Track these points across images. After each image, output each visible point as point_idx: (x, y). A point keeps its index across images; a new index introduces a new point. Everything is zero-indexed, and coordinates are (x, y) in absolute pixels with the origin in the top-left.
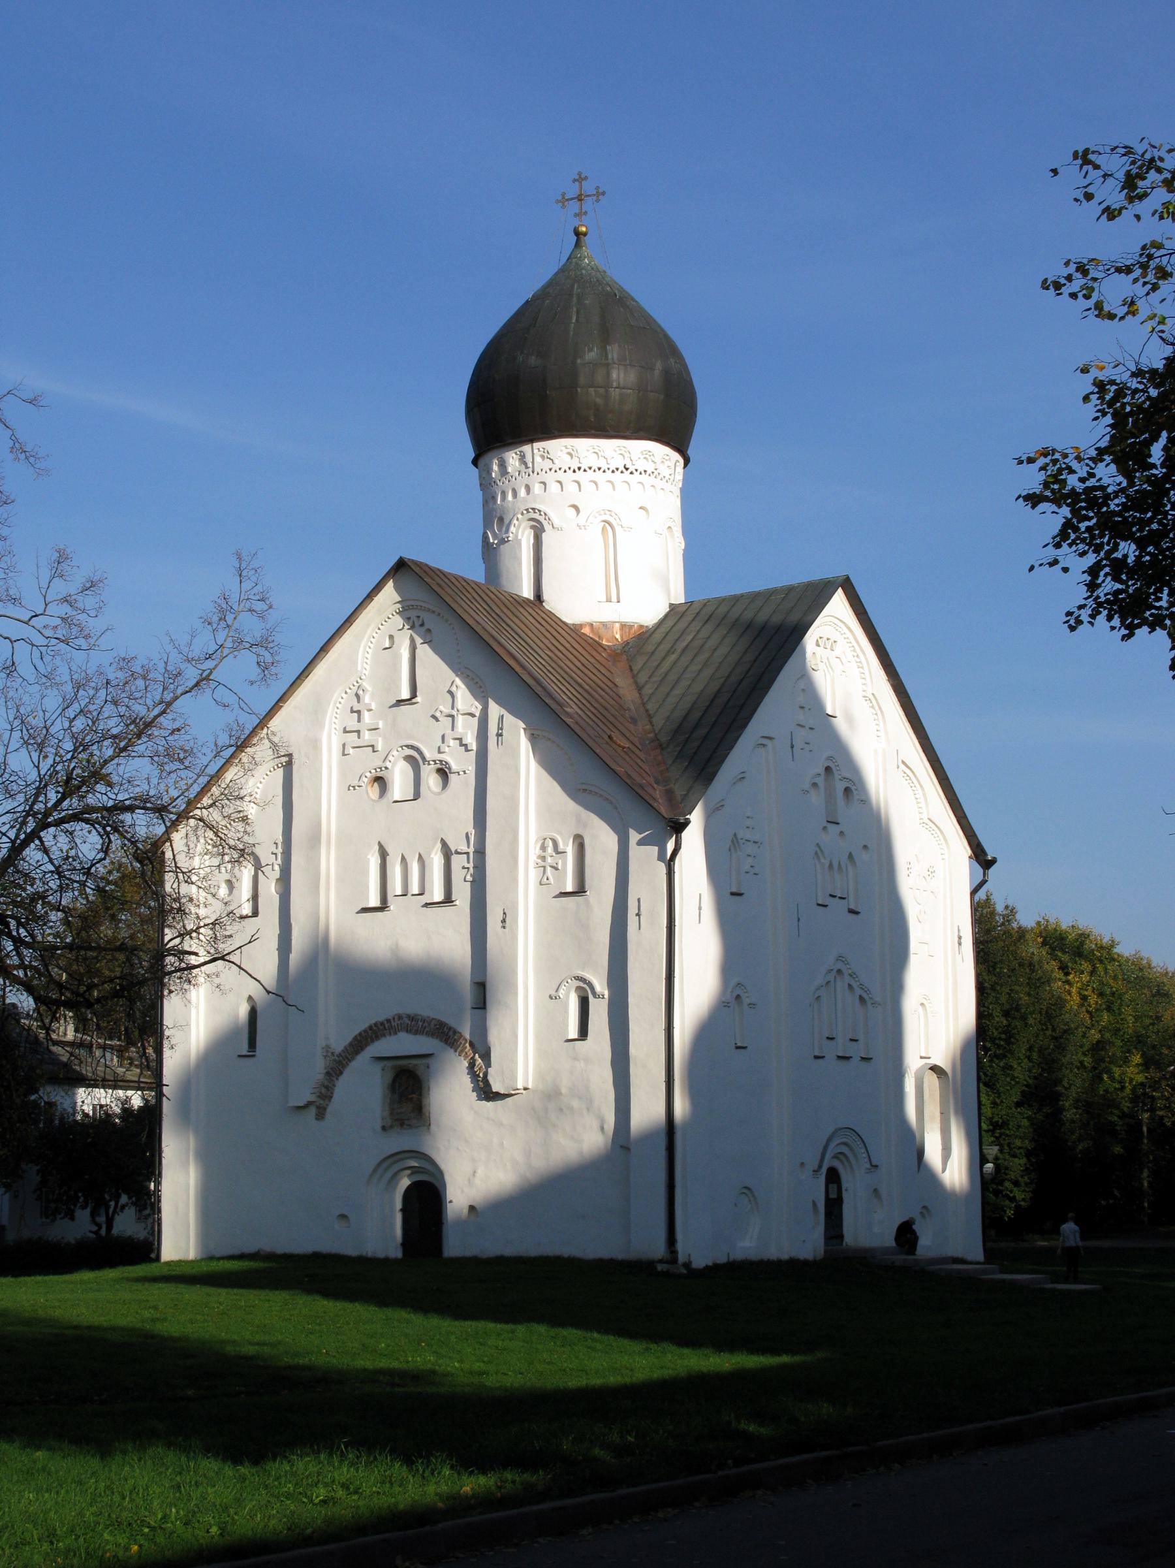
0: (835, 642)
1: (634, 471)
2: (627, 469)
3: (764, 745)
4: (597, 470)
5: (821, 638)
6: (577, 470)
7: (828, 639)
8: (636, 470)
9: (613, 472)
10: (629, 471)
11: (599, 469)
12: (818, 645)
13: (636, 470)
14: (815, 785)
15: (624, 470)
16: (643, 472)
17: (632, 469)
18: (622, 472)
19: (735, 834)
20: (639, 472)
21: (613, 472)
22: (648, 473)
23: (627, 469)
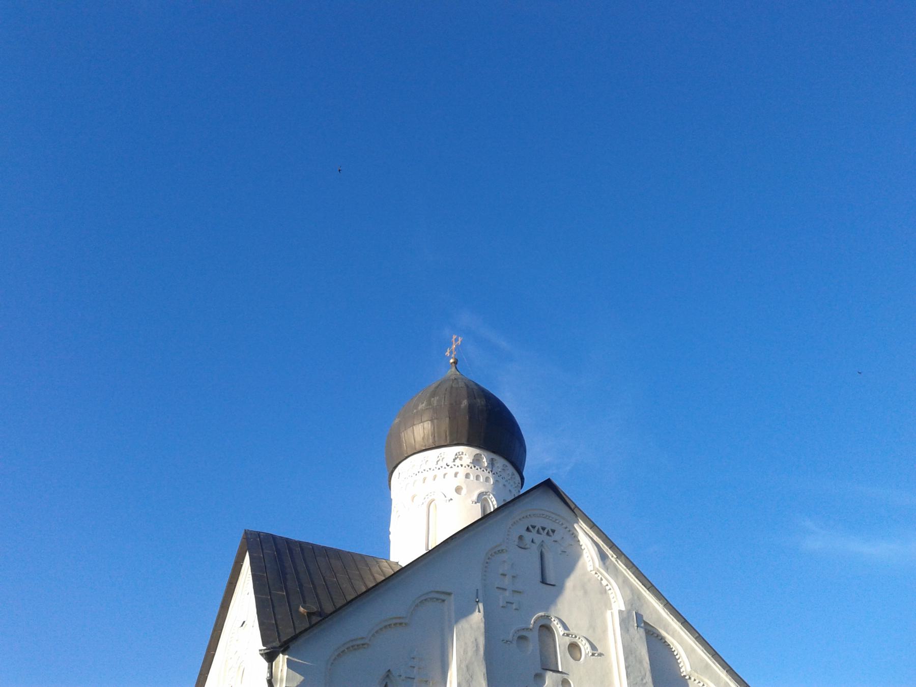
0: (553, 531)
1: (453, 466)
2: (448, 466)
3: (444, 601)
4: (429, 470)
5: (534, 527)
6: (417, 473)
7: (544, 529)
8: (455, 465)
9: (439, 469)
10: (450, 466)
11: (430, 469)
12: (528, 529)
13: (455, 465)
14: (522, 638)
15: (446, 467)
16: (460, 466)
17: (451, 464)
18: (445, 468)
19: (389, 671)
20: (456, 466)
21: (439, 469)
22: (463, 466)
23: (448, 466)
